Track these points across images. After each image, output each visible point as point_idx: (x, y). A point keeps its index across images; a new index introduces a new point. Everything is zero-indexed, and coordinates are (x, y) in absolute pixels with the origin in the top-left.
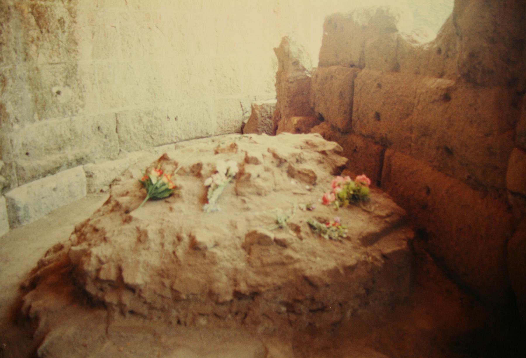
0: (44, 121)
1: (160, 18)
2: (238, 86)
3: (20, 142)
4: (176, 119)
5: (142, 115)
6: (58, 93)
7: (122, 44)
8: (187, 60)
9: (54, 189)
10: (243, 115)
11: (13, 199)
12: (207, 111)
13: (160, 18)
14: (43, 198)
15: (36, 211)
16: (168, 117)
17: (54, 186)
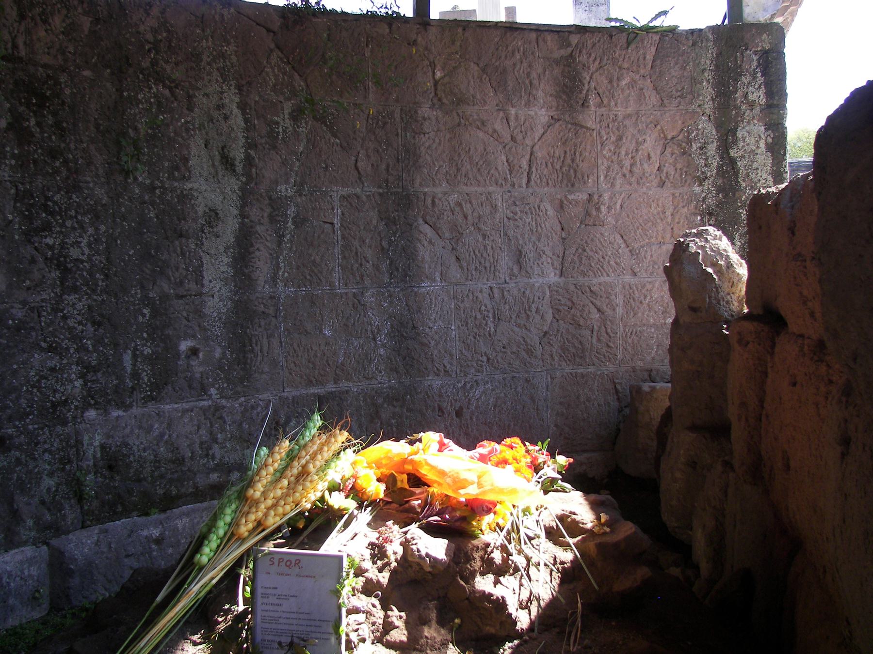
0: (152, 407)
1: (433, 202)
2: (608, 346)
3: (97, 443)
4: (459, 414)
5: (380, 401)
6: (194, 352)
7: (344, 257)
8: (491, 288)
9: (158, 541)
10: (620, 411)
11: (62, 553)
12: (532, 399)
13: (433, 202)
14: (127, 556)
15: (110, 581)
16: (440, 409)
17: (156, 533)
